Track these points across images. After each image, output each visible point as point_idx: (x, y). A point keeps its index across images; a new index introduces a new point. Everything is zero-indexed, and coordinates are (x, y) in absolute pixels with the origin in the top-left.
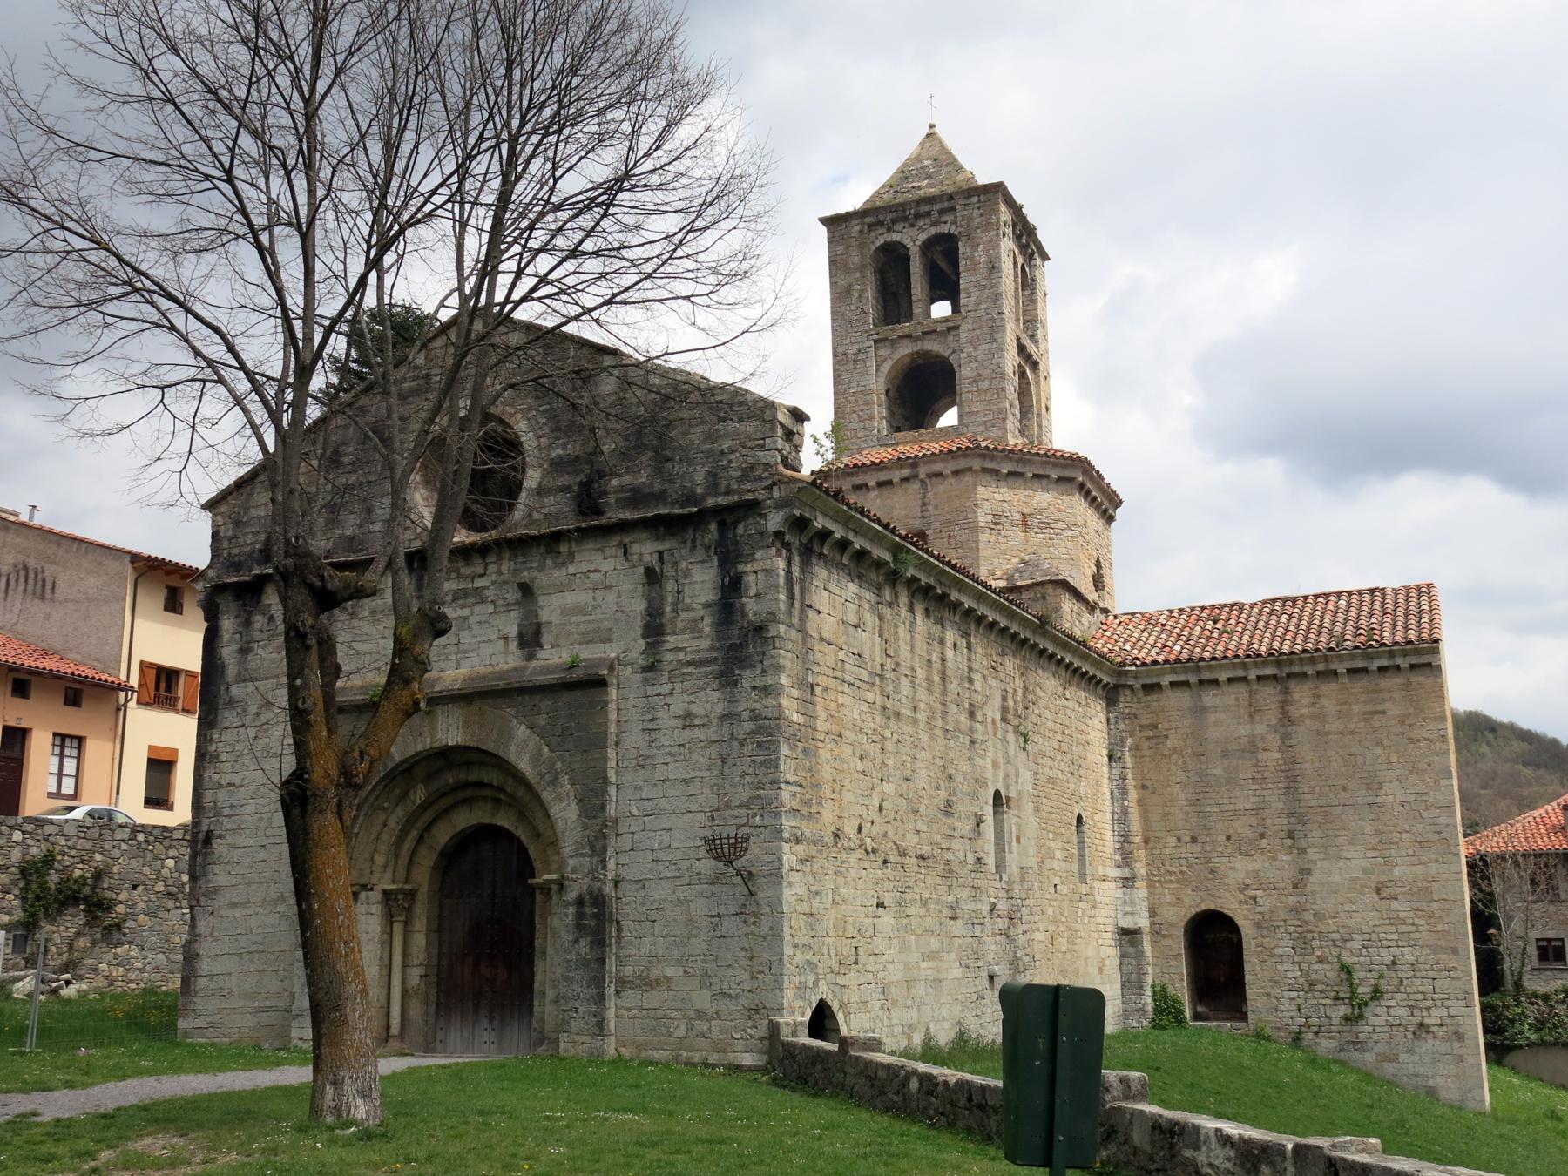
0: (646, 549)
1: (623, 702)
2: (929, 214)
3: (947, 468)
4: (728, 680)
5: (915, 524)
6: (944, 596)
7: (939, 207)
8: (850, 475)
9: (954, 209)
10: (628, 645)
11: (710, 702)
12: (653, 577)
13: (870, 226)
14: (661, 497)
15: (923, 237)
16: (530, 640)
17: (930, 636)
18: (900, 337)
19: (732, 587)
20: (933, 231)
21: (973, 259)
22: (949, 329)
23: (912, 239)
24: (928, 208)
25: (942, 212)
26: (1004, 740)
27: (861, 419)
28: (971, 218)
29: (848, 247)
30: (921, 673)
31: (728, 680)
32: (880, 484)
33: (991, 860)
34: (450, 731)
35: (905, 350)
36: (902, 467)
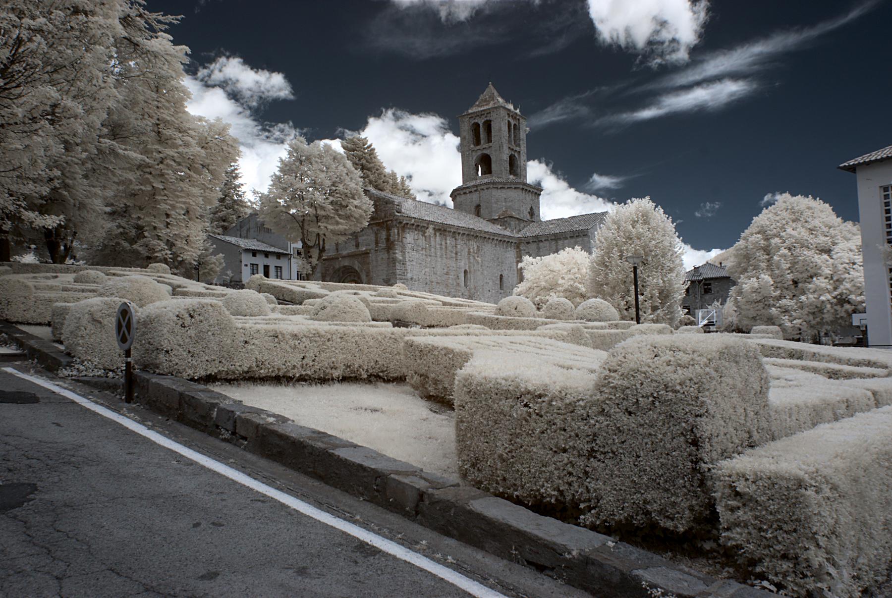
0: (375, 228)
1: (372, 256)
3: (484, 187)
4: (388, 252)
5: (478, 202)
6: (445, 231)
10: (373, 246)
11: (386, 256)
12: (376, 234)
14: (377, 219)
16: (357, 245)
17: (441, 240)
19: (388, 236)
26: (469, 258)
30: (438, 246)
31: (388, 252)
33: (463, 284)
34: (346, 263)
35: (479, 153)
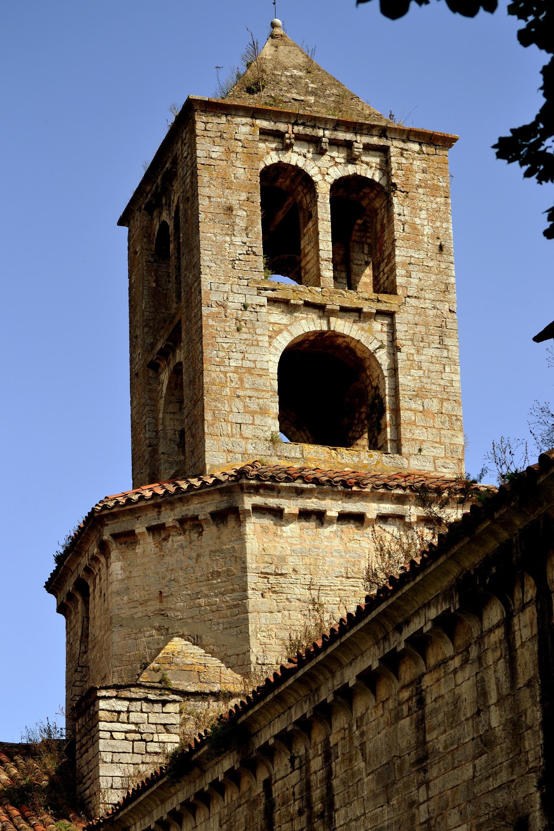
2: (348, 145)
7: (366, 139)
8: (299, 493)
9: (384, 151)
13: (264, 132)
15: (337, 173)
18: (307, 304)
20: (351, 170)
21: (414, 226)
22: (380, 313)
23: (325, 171)
24: (349, 136)
25: (368, 148)
27: (247, 411)
28: (409, 170)
29: (229, 151)
32: (344, 517)
35: (309, 324)
36: (381, 499)
